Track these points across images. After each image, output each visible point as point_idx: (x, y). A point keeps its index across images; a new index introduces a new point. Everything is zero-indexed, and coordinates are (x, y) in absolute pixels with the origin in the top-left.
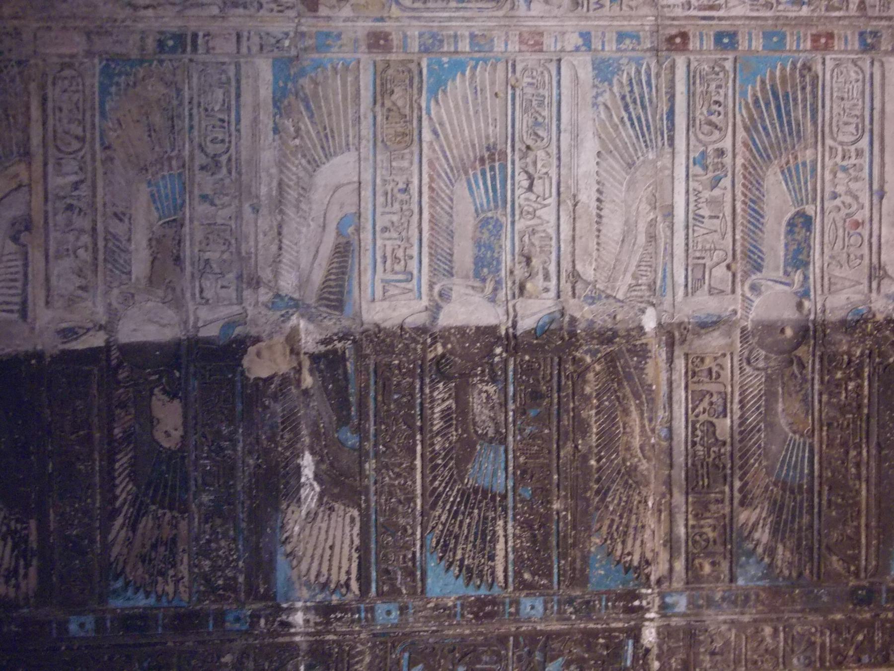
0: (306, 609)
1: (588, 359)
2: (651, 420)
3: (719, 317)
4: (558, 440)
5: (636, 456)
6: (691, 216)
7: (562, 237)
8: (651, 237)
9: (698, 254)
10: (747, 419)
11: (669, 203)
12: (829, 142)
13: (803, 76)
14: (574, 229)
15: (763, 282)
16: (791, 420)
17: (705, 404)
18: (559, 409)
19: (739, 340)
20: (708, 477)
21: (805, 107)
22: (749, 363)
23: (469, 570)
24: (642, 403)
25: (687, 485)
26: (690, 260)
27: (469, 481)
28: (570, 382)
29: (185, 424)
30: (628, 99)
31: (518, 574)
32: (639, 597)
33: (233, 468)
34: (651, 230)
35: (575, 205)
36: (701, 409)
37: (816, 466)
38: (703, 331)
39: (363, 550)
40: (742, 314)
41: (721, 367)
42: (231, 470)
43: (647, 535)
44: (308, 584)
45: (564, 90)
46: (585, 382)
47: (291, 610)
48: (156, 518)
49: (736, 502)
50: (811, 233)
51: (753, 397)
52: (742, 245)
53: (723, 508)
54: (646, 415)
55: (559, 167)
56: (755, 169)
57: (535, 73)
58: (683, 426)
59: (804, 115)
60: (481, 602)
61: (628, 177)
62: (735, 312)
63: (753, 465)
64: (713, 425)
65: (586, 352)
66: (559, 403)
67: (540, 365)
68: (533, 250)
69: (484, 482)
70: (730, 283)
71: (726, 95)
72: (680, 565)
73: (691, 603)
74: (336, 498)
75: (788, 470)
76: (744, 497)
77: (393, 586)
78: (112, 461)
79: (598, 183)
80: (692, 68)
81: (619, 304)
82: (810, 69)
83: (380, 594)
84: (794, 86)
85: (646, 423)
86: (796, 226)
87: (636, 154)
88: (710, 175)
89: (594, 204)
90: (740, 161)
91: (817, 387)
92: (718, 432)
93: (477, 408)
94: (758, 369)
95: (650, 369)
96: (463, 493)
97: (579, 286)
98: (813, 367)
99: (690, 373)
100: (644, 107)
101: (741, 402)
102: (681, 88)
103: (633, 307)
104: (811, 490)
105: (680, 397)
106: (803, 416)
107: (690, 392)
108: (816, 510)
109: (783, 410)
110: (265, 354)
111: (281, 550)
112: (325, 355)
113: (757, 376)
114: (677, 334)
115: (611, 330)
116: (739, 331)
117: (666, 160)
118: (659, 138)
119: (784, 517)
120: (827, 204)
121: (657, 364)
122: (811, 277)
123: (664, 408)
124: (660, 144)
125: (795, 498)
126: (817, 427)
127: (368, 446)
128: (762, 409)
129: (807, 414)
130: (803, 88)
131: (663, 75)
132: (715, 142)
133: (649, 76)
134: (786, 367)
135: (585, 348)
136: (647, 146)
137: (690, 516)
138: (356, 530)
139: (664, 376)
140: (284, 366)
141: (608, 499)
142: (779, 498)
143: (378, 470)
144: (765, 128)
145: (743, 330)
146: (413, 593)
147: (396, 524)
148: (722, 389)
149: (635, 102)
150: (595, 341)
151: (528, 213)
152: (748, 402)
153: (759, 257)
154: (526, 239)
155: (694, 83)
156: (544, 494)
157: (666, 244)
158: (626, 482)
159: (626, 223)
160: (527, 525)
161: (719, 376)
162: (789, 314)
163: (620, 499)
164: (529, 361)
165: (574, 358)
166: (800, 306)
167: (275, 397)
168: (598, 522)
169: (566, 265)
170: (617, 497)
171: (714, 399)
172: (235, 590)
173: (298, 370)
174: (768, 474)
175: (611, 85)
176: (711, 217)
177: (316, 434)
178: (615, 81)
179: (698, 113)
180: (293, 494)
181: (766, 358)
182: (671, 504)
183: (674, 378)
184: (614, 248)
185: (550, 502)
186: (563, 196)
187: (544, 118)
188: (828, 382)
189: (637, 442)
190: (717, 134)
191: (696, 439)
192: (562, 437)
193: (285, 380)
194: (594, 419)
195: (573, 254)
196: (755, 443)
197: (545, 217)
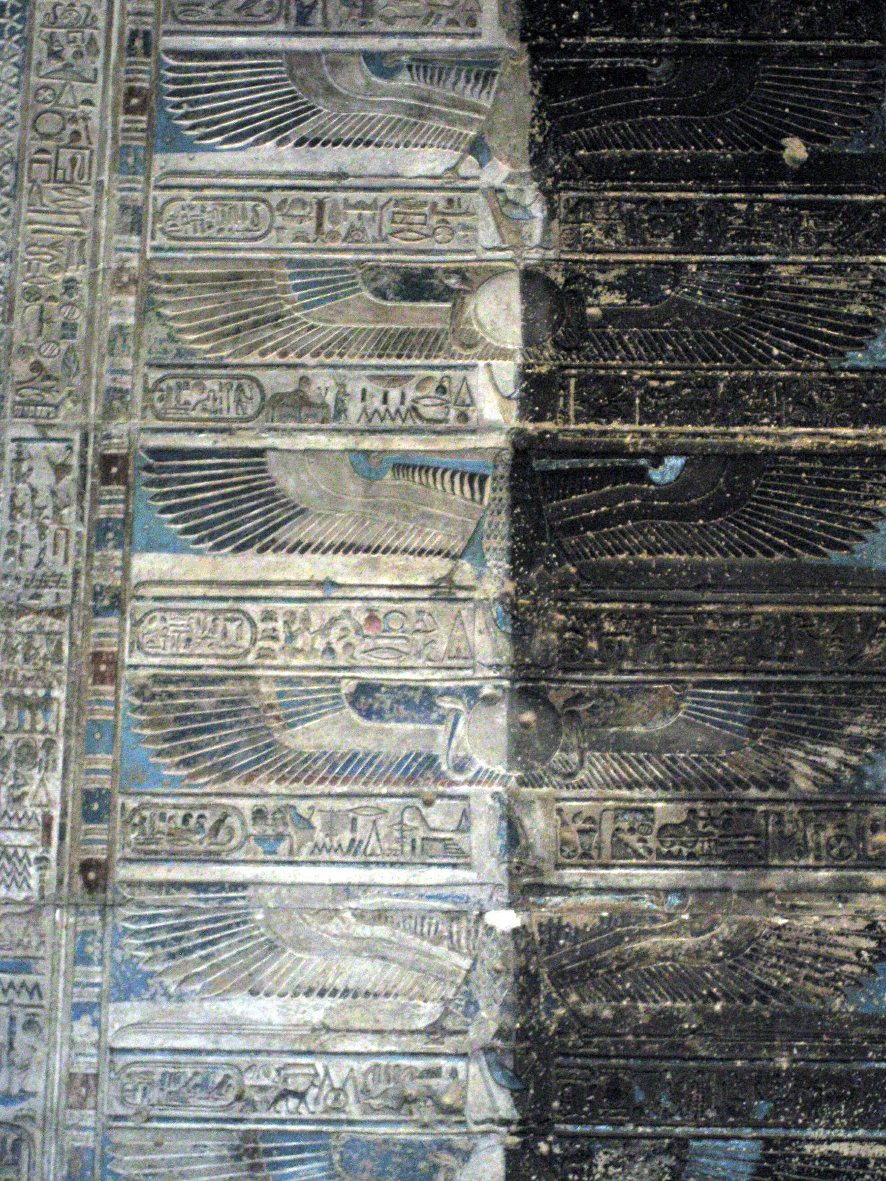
1: (561, 1011)
2: (655, 920)
3: (502, 818)
4: (684, 1059)
5: (710, 943)
6: (349, 858)
7: (374, 1048)
8: (380, 917)
9: (407, 848)
10: (656, 778)
11: (329, 891)
12: (251, 659)
13: (153, 696)
14: (364, 1031)
15: (451, 753)
16: (659, 715)
17: (632, 839)
18: (635, 1058)
19: (538, 790)
20: (744, 835)
21: (198, 694)
22: (571, 775)
24: (629, 933)
25: (752, 866)
26: (415, 860)
28: (596, 1040)
30: (175, 949)
34: (369, 916)
35: (328, 1029)
36: (639, 846)
37: (729, 677)
38: (523, 842)
40: (500, 784)
41: (577, 814)
45: (157, 1043)
46: (595, 1017)
49: (781, 795)
50: (381, 685)
51: (623, 768)
52: (396, 783)
53: (791, 813)
54: (647, 927)
55: (269, 1053)
56: (285, 765)
57: (129, 1087)
58: (666, 872)
59: (211, 694)
61: (290, 950)
62: (495, 795)
63: (724, 769)
64: (663, 828)
65: (550, 1014)
66: (627, 1057)
67: (566, 1085)
68: (391, 1093)
70: (453, 802)
71: (175, 807)
75: (734, 719)
76: (773, 782)
79: (295, 995)
80: (133, 856)
81: (478, 965)
82: (144, 687)
84: (165, 709)
85: (659, 926)
86: (371, 705)
87: (256, 937)
88: (291, 830)
89: (327, 1002)
90: (273, 787)
91: (610, 677)
92: (675, 821)
94: (582, 761)
95: (579, 920)
97: (449, 1024)
99: (585, 861)
100: (187, 926)
101: (629, 787)
102: (161, 873)
103: (484, 943)
104: (764, 686)
105: (620, 875)
106: (653, 696)
107: (614, 861)
108: (794, 678)
109: (644, 725)
113: (591, 763)
114: (526, 880)
115: (517, 978)
116: (524, 790)
117: (267, 894)
118: (234, 903)
119: (804, 724)
120: (342, 663)
121: (570, 910)
122: (447, 684)
123: (636, 899)
124: (241, 903)
125: (775, 708)
126: (670, 677)
128: (641, 755)
129: (649, 691)
130: (171, 695)
131: (142, 898)
132: (243, 823)
133: (142, 918)
134: (580, 722)
135: (543, 1017)
136: (245, 922)
137: (802, 862)
139: (588, 899)
141: (775, 984)
142: (774, 732)
144: (227, 751)
145: (522, 782)
148: (610, 814)
149: (178, 940)
150: (534, 1002)
151: (336, 1099)
152: (630, 775)
153: (414, 760)
154: (375, 1103)
155: (156, 852)
157: (390, 895)
158: (749, 957)
159: (356, 953)
161: (590, 819)
162: (500, 717)
163: (774, 966)
164: (562, 1102)
165: (558, 1033)
166: (490, 701)
168: (809, 1001)
169: (419, 1044)
170: (771, 970)
171: (625, 826)
174: (736, 746)
175: (151, 975)
176: (354, 829)
178: (147, 968)
179: (201, 848)
181: (565, 749)
182: (783, 891)
183: (591, 885)
184: (393, 972)
185: (778, 1072)
186: (313, 1046)
187: (196, 1074)
188: (603, 660)
189: (688, 941)
190: (233, 821)
191: (685, 851)
192: (678, 1051)
194: (652, 1005)
195: (401, 1033)
196: (693, 767)
197: (345, 1072)
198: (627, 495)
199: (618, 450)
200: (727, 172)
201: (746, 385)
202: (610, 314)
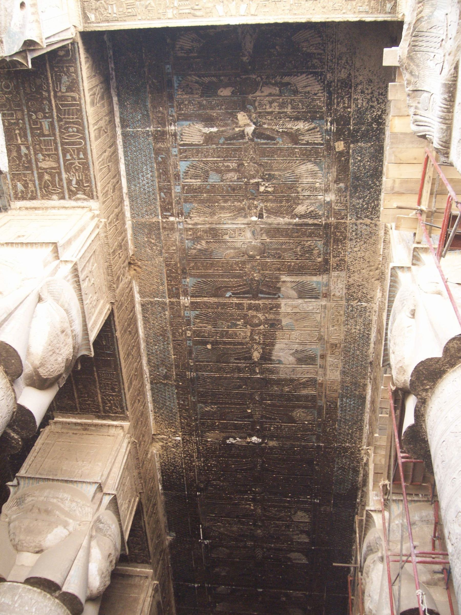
0: (175, 130)
17: (232, 233)
23: (187, 173)
27: (211, 172)
29: (225, 96)
31: (186, 185)
32: (182, 216)
33: (213, 109)
39: (191, 145)
42: (212, 109)
43: (198, 218)
44: (182, 130)
47: (175, 126)
48: (199, 89)
60: (179, 176)
69: (210, 176)
72: (190, 226)
73: (181, 230)
74: (205, 137)
77: (182, 153)
78: (213, 76)
83: (180, 149)
93: (230, 174)
96: (207, 171)
98: (243, 259)
110: (244, 118)
111: (191, 123)
112: (244, 134)
127: (220, 146)
138: (197, 143)
139: (239, 222)
140: (241, 123)
143: (213, 148)
146: (181, 158)
147: (198, 153)
156: (208, 192)
160: (199, 188)
167: (232, 121)
172: (180, 110)
173: (240, 127)
177: (223, 132)
180: (206, 126)
189: (222, 215)
192: (223, 196)
193: (237, 123)
198: (235, 290)
199: (237, 297)
200: (220, 343)
201: (216, 308)
202: (239, 320)
